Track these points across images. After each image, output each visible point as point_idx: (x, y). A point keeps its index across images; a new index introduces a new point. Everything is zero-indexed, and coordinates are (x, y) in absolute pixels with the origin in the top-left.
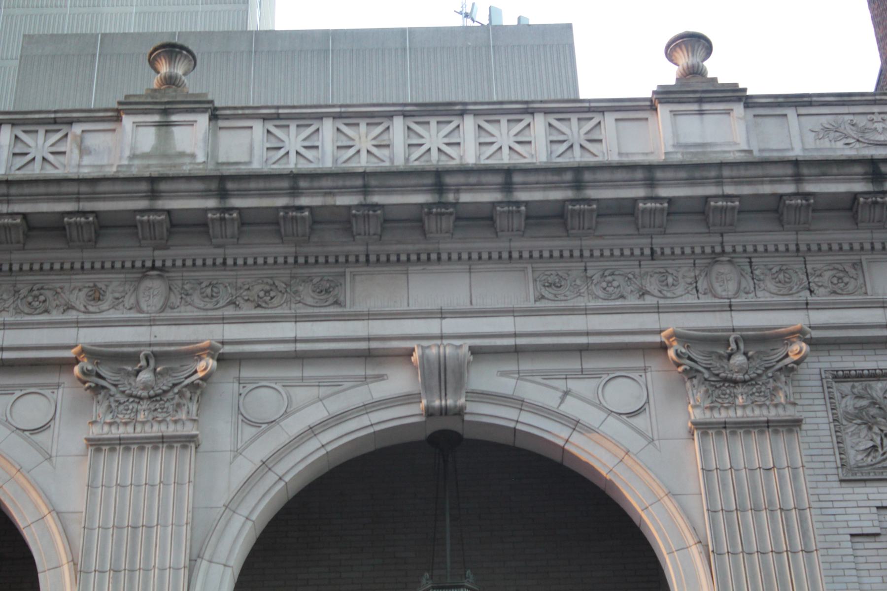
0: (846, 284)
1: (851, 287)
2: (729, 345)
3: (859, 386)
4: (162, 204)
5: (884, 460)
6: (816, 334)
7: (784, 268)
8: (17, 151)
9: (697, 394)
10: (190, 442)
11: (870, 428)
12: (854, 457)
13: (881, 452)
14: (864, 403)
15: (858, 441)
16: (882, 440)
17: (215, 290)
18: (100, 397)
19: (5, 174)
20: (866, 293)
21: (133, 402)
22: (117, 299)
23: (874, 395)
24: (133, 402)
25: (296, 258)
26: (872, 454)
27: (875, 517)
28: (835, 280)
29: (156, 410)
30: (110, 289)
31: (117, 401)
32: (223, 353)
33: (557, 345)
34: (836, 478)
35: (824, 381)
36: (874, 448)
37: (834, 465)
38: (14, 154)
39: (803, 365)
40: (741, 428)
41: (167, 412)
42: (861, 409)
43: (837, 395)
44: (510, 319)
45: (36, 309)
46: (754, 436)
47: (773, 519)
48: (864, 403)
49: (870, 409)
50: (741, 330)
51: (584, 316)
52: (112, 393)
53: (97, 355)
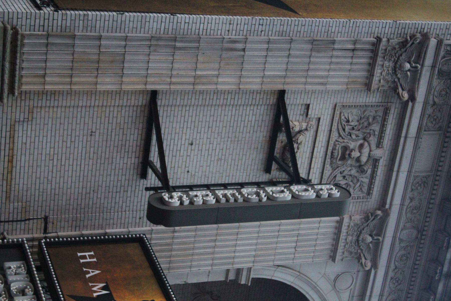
0: (432, 122)
1: (430, 124)
2: (415, 63)
3: (380, 119)
5: (341, 125)
6: (410, 104)
7: (448, 95)
9: (395, 41)
11: (358, 121)
12: (346, 113)
13: (346, 124)
14: (371, 120)
15: (353, 115)
16: (351, 125)
20: (425, 131)
23: (374, 125)
26: (345, 120)
27: (316, 116)
28: (435, 117)
33: (403, 124)
34: (338, 101)
35: (386, 104)
36: (348, 121)
37: (345, 101)
39: (396, 96)
42: (368, 119)
43: (378, 109)
44: (414, 135)
46: (364, 74)
47: (325, 70)
48: (371, 120)
49: (367, 122)
50: (421, 71)
51: (407, 170)
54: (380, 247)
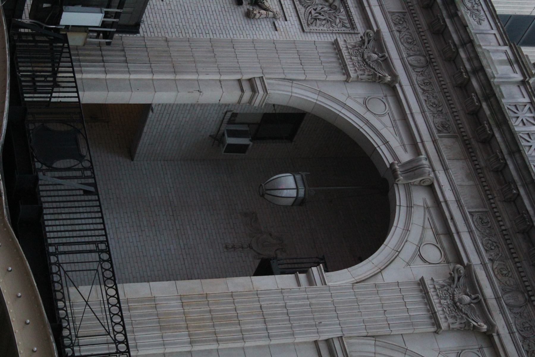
4: (495, 130)
8: (518, 106)
10: (437, 326)
17: (529, 328)
18: (448, 281)
19: (516, 131)
21: (450, 296)
22: (506, 283)
24: (450, 296)
25: (505, 230)
29: (449, 308)
30: (510, 279)
31: (448, 289)
32: (493, 336)
38: (515, 106)
40: (435, 320)
41: (450, 313)
45: (486, 246)
52: (452, 286)
53: (468, 268)
54: (484, 305)
